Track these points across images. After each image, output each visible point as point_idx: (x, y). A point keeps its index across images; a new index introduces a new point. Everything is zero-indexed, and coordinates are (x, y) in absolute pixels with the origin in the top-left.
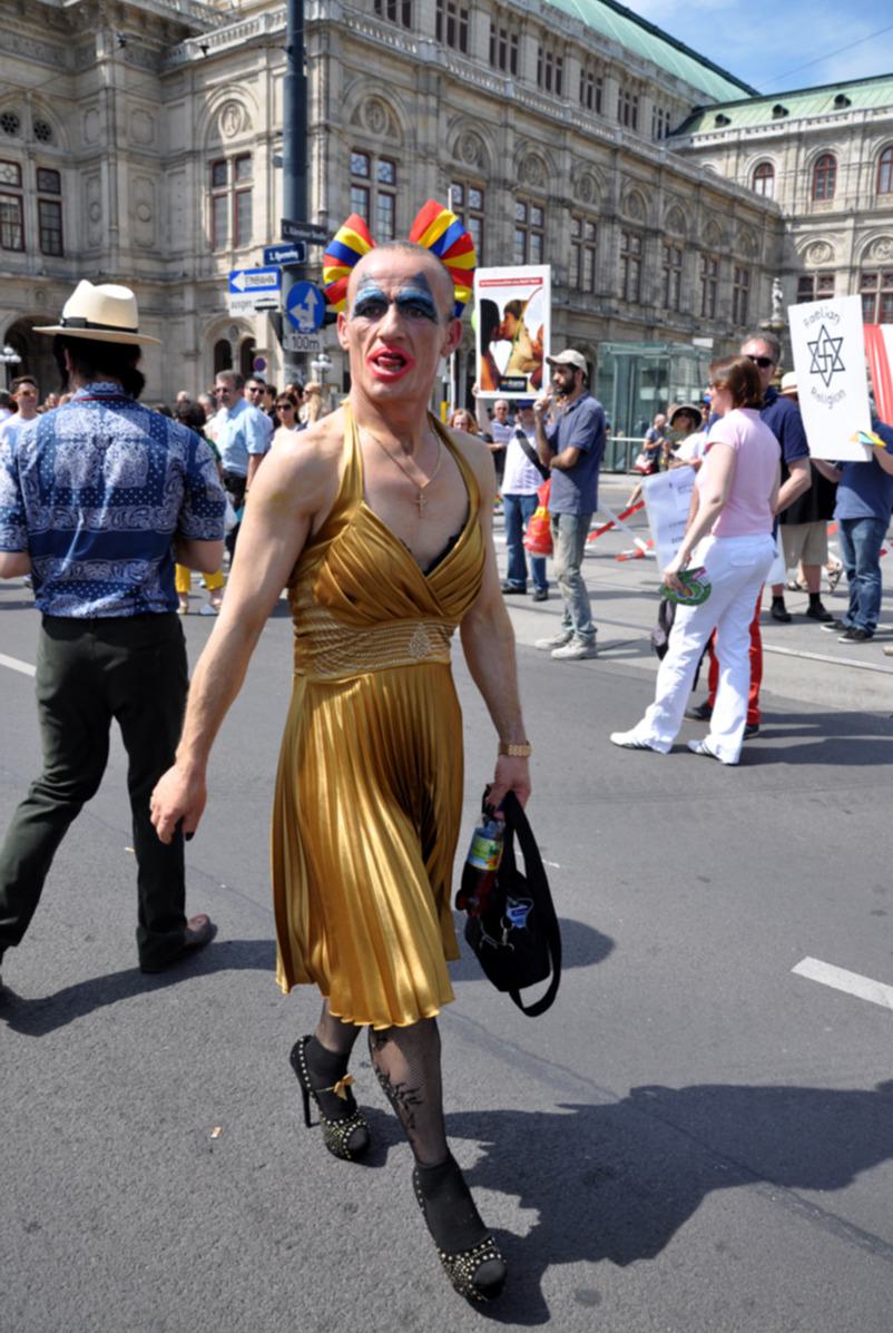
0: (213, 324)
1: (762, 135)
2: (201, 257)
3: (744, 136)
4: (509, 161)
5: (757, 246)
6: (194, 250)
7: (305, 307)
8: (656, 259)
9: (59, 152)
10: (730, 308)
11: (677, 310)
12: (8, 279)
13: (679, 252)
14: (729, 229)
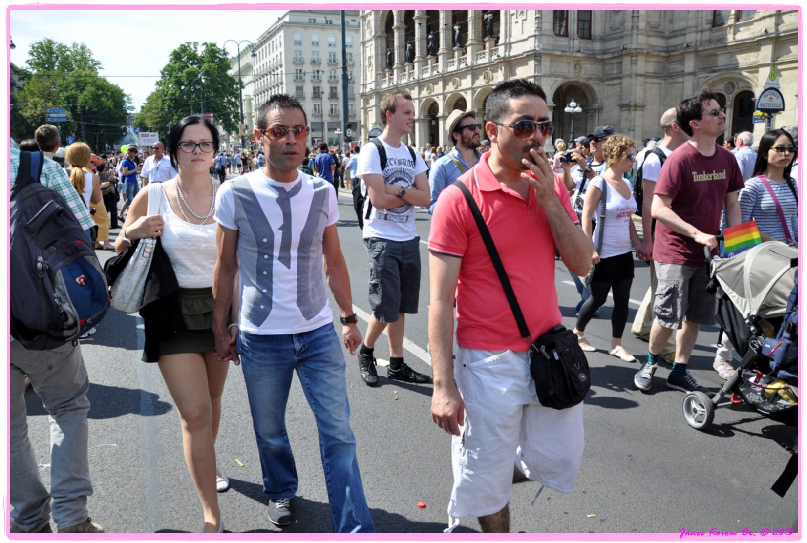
0: (710, 82)
2: (702, 31)
6: (696, 27)
12: (558, 56)
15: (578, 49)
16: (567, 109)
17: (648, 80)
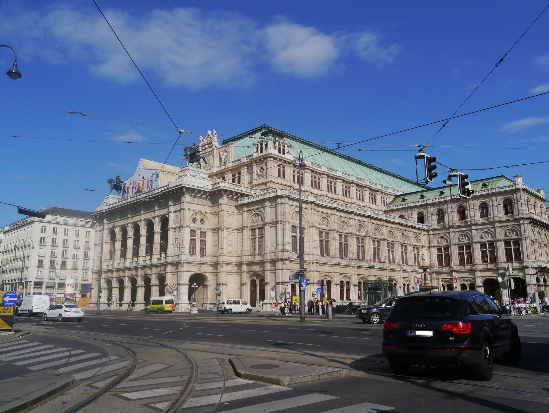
1: (418, 204)
3: (412, 205)
4: (336, 224)
5: (420, 239)
7: (304, 282)
8: (384, 247)
9: (206, 227)
10: (413, 261)
11: (394, 263)
13: (392, 244)
14: (409, 235)
15: (200, 260)
16: (193, 286)
17: (228, 273)
